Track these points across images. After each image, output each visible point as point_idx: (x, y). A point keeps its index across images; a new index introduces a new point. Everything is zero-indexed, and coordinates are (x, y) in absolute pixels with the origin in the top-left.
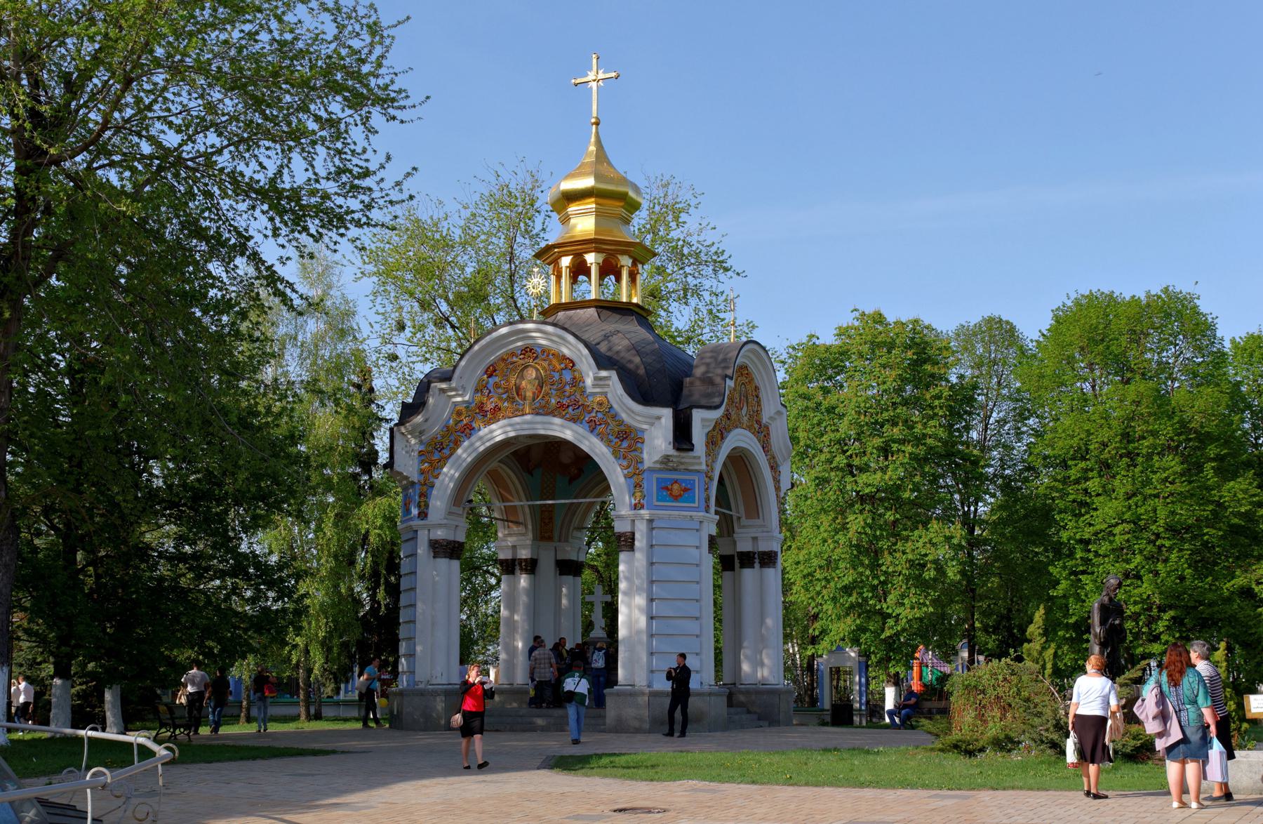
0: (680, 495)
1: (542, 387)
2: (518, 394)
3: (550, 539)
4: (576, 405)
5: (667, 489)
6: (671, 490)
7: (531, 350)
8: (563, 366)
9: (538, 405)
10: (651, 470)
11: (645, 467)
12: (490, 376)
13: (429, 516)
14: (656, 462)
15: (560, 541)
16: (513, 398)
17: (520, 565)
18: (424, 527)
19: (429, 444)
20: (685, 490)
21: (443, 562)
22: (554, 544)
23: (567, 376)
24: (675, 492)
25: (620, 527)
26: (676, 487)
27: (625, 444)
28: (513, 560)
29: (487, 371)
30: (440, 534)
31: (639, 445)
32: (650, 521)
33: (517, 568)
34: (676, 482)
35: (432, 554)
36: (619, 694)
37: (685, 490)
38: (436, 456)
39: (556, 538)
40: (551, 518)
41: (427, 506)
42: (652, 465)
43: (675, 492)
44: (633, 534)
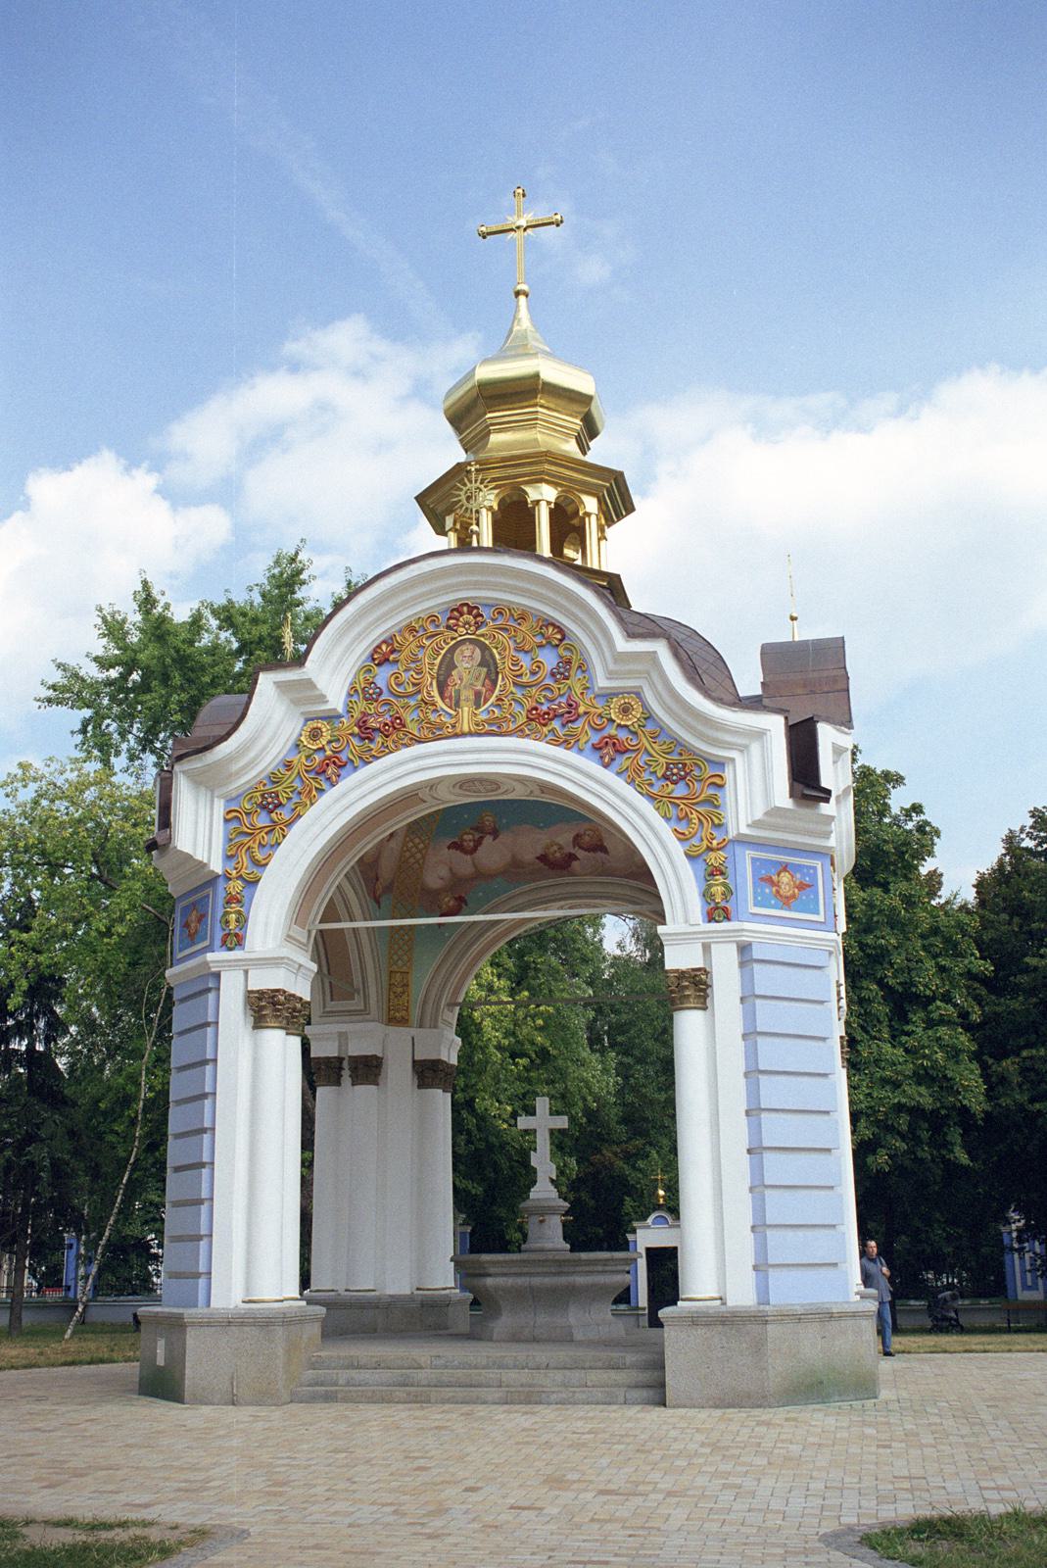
0: (793, 896)
1: (494, 683)
3: (403, 1022)
4: (571, 714)
6: (777, 884)
7: (471, 609)
8: (538, 640)
9: (484, 717)
10: (743, 841)
11: (732, 834)
12: (378, 665)
14: (756, 824)
17: (354, 1070)
18: (232, 964)
20: (802, 887)
22: (414, 1031)
23: (549, 659)
24: (786, 890)
25: (678, 958)
26: (785, 878)
28: (340, 1060)
29: (375, 651)
30: (265, 980)
32: (744, 949)
33: (346, 1073)
34: (785, 868)
36: (695, 1320)
37: (802, 887)
38: (262, 820)
41: (242, 920)
42: (744, 830)
43: (786, 890)
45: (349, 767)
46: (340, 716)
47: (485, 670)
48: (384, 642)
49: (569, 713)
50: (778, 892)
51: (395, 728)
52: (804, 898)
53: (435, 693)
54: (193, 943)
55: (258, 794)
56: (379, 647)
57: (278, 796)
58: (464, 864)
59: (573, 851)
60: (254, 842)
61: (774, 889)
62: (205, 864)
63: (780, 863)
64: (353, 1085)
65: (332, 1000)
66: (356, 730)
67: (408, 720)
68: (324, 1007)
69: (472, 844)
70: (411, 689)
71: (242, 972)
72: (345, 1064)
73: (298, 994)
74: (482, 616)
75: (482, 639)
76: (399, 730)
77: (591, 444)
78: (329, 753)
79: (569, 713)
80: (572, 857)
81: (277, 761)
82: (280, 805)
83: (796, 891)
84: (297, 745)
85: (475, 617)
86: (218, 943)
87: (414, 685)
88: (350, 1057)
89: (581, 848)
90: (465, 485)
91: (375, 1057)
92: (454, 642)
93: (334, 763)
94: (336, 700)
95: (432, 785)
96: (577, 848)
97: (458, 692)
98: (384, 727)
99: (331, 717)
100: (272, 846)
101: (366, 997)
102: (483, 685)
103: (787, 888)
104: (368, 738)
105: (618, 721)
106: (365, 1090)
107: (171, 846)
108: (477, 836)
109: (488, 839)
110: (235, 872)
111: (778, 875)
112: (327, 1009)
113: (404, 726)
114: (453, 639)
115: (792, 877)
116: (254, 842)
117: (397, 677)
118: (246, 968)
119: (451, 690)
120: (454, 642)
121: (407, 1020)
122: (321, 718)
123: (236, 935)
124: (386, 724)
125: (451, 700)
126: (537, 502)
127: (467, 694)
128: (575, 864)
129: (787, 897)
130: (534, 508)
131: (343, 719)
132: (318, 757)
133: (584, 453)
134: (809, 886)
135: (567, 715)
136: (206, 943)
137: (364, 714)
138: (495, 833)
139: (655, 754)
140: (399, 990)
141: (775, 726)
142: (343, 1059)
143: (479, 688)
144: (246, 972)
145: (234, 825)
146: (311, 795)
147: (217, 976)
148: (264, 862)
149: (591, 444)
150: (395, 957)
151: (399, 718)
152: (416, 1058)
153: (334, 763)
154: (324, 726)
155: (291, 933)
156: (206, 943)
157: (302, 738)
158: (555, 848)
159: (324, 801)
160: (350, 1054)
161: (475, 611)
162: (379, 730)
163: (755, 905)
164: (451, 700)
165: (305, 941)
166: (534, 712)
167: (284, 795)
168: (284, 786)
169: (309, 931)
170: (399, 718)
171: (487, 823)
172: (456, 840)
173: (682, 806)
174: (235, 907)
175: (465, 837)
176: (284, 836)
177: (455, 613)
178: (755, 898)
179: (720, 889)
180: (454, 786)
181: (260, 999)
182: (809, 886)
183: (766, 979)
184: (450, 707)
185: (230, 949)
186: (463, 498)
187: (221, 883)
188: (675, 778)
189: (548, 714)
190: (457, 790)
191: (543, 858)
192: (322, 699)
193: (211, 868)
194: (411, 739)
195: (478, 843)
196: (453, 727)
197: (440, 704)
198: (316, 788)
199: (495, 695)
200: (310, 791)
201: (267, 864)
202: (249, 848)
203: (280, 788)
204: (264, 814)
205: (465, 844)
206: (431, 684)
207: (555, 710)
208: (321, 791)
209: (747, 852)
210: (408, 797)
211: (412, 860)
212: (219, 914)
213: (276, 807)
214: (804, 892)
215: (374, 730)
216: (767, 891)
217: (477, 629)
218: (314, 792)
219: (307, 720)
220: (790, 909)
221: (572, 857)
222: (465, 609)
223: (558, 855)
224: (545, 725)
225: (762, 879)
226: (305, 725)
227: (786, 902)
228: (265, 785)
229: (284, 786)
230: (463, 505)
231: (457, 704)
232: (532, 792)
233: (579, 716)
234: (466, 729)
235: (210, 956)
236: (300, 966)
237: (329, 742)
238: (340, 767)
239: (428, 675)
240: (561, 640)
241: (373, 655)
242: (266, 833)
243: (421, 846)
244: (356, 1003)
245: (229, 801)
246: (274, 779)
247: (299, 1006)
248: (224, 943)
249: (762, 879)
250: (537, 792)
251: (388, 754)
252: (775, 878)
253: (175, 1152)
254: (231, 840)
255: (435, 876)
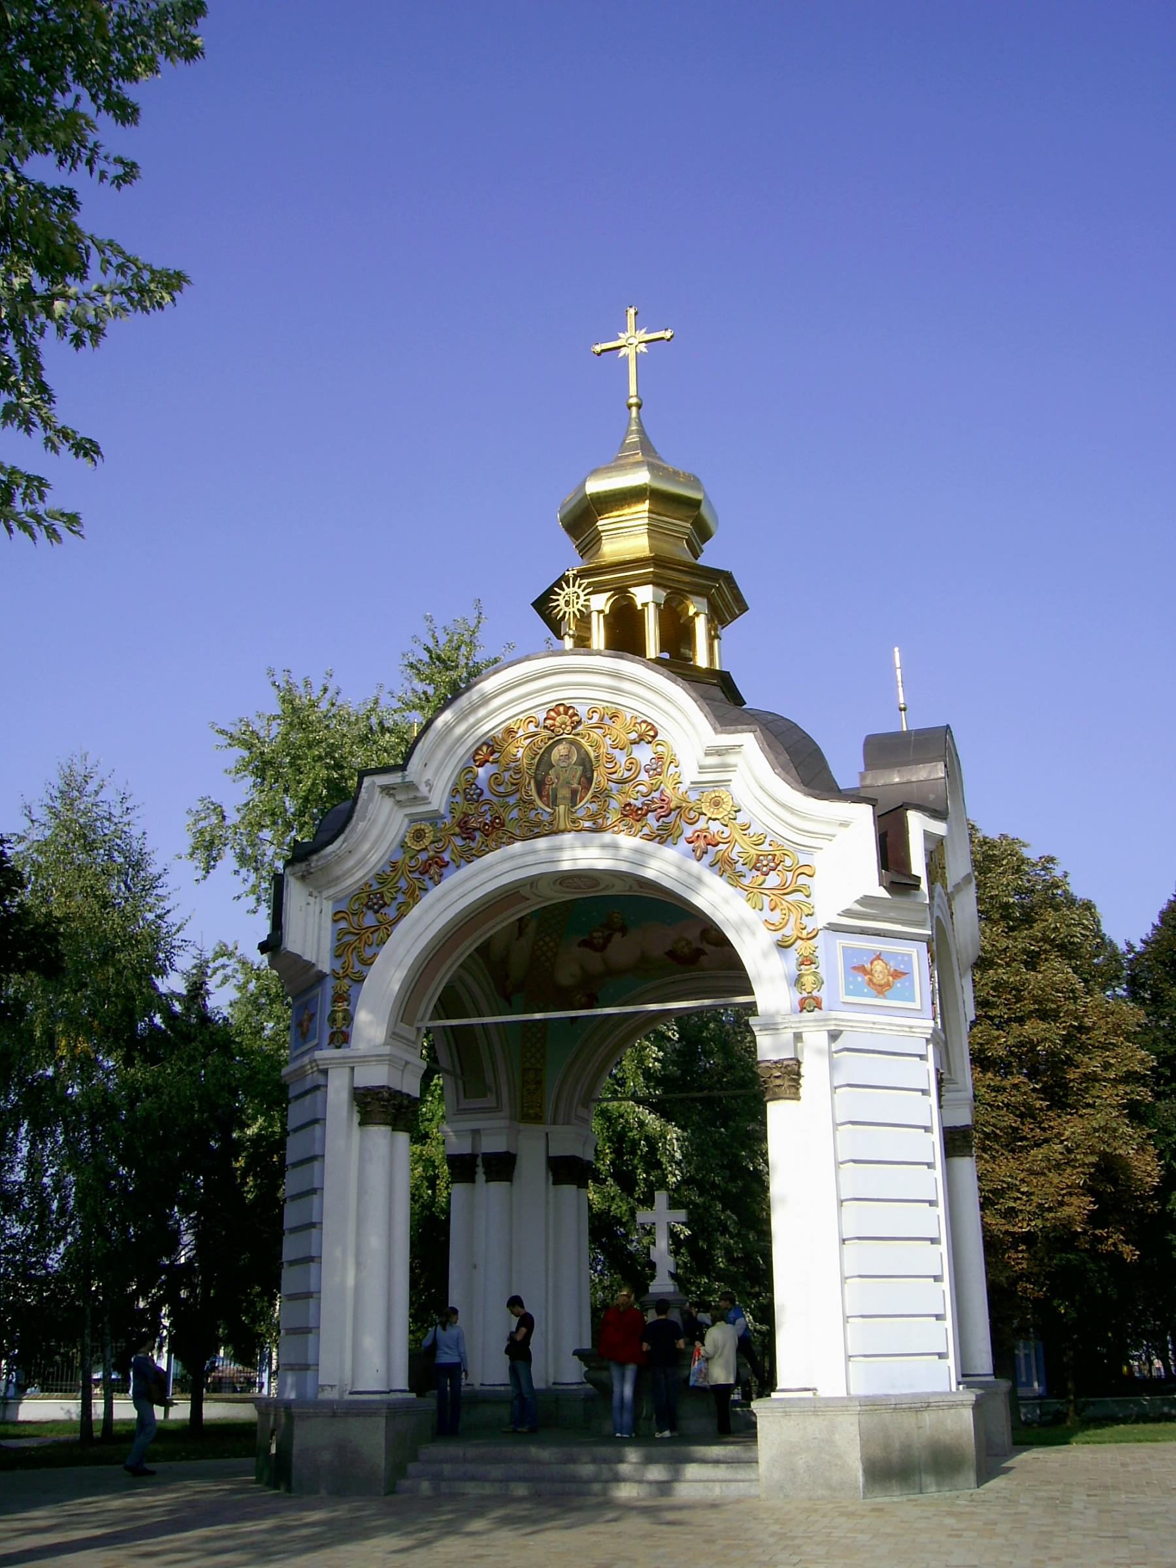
0: (888, 985)
2: (540, 796)
3: (537, 1118)
5: (861, 969)
13: (353, 1041)
15: (554, 1123)
16: (532, 802)
19: (355, 897)
20: (897, 974)
21: (379, 1134)
24: (879, 978)
26: (878, 966)
27: (773, 880)
28: (473, 1157)
29: (476, 753)
31: (802, 880)
33: (480, 1170)
35: (356, 1118)
37: (897, 974)
38: (370, 919)
39: (549, 1114)
40: (539, 1083)
43: (879, 978)
44: (799, 1063)
45: (452, 866)
46: (443, 817)
47: (581, 768)
48: (484, 743)
49: (662, 807)
50: (870, 980)
51: (495, 828)
52: (899, 985)
53: (534, 792)
54: (305, 1042)
55: (364, 895)
56: (479, 748)
57: (382, 897)
58: (594, 962)
59: (700, 946)
60: (360, 943)
61: (867, 978)
62: (314, 964)
63: (874, 951)
64: (487, 1181)
65: (465, 1097)
66: (457, 830)
67: (507, 821)
68: (458, 1104)
69: (601, 941)
70: (511, 788)
71: (347, 1070)
72: (479, 1161)
73: (405, 1090)
74: (577, 715)
75: (578, 738)
76: (498, 829)
77: (703, 546)
78: (431, 853)
79: (662, 807)
80: (700, 952)
81: (382, 863)
82: (385, 904)
83: (891, 979)
84: (403, 845)
85: (571, 717)
86: (326, 1040)
87: (513, 784)
88: (483, 1154)
89: (709, 943)
90: (563, 590)
91: (507, 1153)
92: (551, 741)
93: (436, 863)
94: (438, 799)
95: (533, 881)
96: (704, 943)
97: (555, 791)
98: (484, 826)
99: (434, 818)
100: (378, 945)
101: (498, 1097)
102: (579, 784)
103: (881, 976)
104: (469, 838)
105: (709, 815)
106: (497, 1187)
107: (282, 947)
108: (607, 933)
109: (617, 937)
110: (341, 971)
111: (872, 963)
112: (460, 1107)
113: (503, 825)
114: (550, 739)
115: (886, 964)
116: (360, 943)
117: (497, 778)
118: (351, 1065)
119: (549, 789)
120: (551, 741)
121: (541, 1117)
122: (421, 820)
123: (343, 1033)
124: (486, 824)
125: (548, 799)
126: (645, 605)
127: (564, 793)
128: (703, 958)
129: (880, 986)
130: (643, 610)
131: (445, 820)
132: (423, 857)
133: (696, 557)
134: (905, 974)
135: (659, 810)
136: (316, 1041)
137: (466, 815)
138: (624, 930)
139: (746, 847)
140: (532, 1087)
141: (862, 817)
142: (477, 1156)
143: (575, 786)
144: (352, 1069)
145: (343, 925)
146: (414, 895)
147: (325, 1072)
148: (369, 962)
149: (703, 546)
150: (528, 1055)
151: (498, 818)
152: (550, 1155)
153: (436, 863)
154: (426, 826)
155: (397, 1030)
156: (316, 1041)
157: (407, 840)
158: (683, 943)
159: (427, 899)
160: (484, 1151)
161: (571, 711)
162: (479, 829)
163: (846, 994)
164: (548, 799)
165: (413, 1038)
166: (628, 808)
167: (389, 895)
168: (389, 886)
169: (419, 1029)
170: (498, 818)
171: (615, 920)
172: (586, 937)
173: (773, 897)
174: (343, 1005)
175: (595, 934)
176: (389, 936)
177: (552, 713)
178: (847, 988)
179: (811, 978)
180: (554, 883)
181: (365, 1096)
182: (905, 974)
183: (856, 1067)
184: (548, 807)
185: (339, 1047)
186: (562, 603)
187: (330, 983)
188: (765, 869)
189: (641, 809)
190: (558, 887)
191: (671, 954)
192: (425, 800)
193: (320, 968)
194: (510, 837)
195: (608, 939)
196: (551, 824)
197: (539, 802)
198: (420, 888)
199: (590, 792)
200: (414, 891)
201: (372, 963)
202: (355, 948)
203: (384, 889)
204: (370, 913)
205: (595, 941)
206: (529, 783)
207: (648, 805)
208: (426, 890)
209: (838, 941)
210: (509, 896)
211: (543, 958)
212: (328, 1012)
213: (382, 906)
214: (898, 980)
215: (476, 829)
216: (860, 979)
217: (573, 728)
218: (417, 893)
219: (411, 821)
220: (885, 997)
221: (700, 952)
222: (561, 709)
223: (686, 950)
224: (638, 821)
225: (854, 968)
226: (409, 827)
227: (881, 989)
228: (371, 886)
229: (389, 886)
230: (565, 612)
231: (554, 803)
232: (631, 887)
233: (672, 810)
234: (562, 827)
235: (318, 1054)
236: (407, 1063)
237: (432, 842)
238: (442, 867)
239: (526, 775)
240: (654, 737)
241: (474, 757)
242: (372, 933)
243: (552, 944)
244: (489, 1101)
245: (337, 901)
246: (381, 878)
247: (406, 1102)
248: (331, 1042)
249: (854, 968)
250: (636, 887)
251: (488, 853)
252: (868, 966)
253: (290, 1248)
254: (339, 940)
255: (567, 975)
